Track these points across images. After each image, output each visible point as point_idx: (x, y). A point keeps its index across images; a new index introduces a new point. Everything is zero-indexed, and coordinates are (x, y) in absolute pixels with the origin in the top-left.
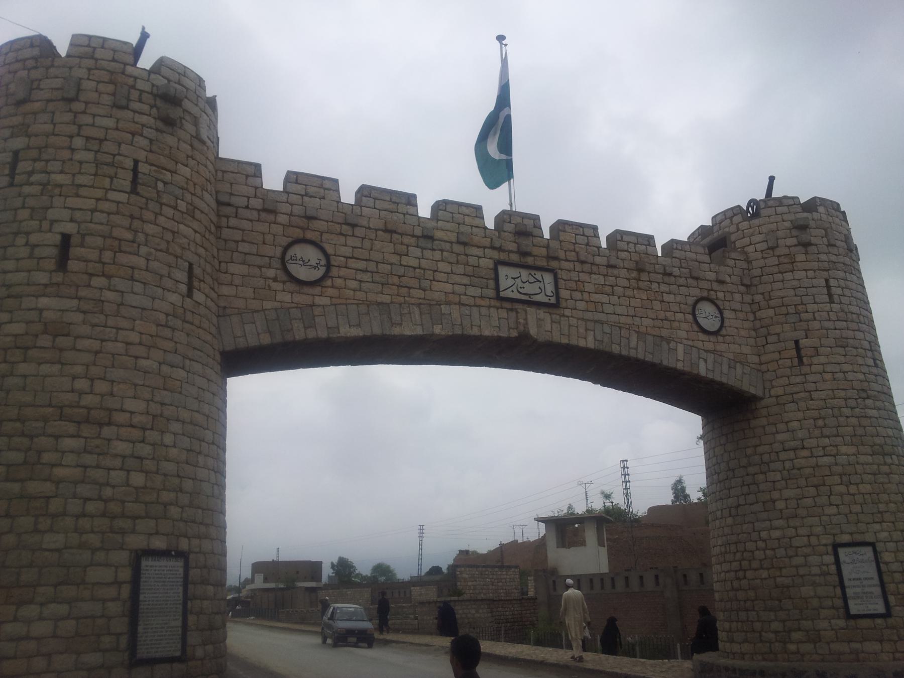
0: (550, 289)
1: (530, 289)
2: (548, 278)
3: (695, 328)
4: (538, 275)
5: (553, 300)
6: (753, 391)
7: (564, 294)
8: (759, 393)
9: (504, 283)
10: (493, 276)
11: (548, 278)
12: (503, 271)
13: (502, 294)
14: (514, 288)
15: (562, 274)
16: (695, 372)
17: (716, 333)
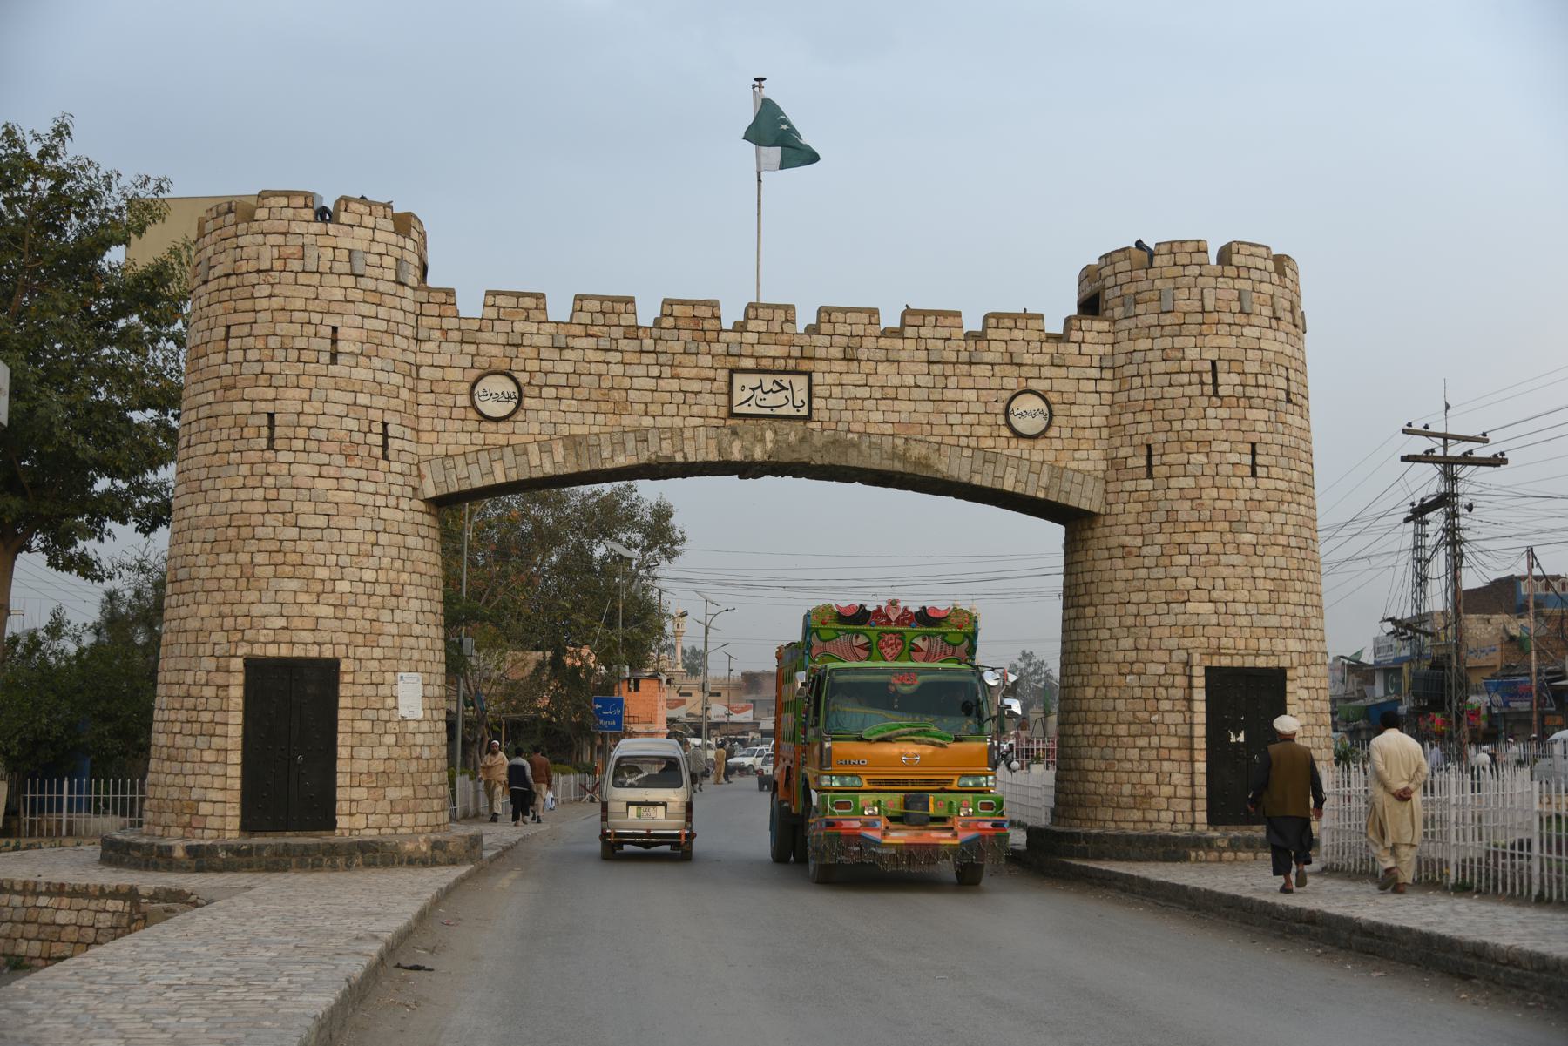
0: (801, 395)
1: (771, 400)
2: (800, 383)
3: (1006, 432)
4: (785, 380)
5: (804, 411)
6: (1084, 505)
7: (817, 403)
8: (1095, 507)
9: (739, 396)
10: (725, 390)
11: (800, 383)
12: (737, 377)
13: (736, 410)
14: (752, 402)
15: (817, 378)
16: (998, 486)
17: (1041, 435)
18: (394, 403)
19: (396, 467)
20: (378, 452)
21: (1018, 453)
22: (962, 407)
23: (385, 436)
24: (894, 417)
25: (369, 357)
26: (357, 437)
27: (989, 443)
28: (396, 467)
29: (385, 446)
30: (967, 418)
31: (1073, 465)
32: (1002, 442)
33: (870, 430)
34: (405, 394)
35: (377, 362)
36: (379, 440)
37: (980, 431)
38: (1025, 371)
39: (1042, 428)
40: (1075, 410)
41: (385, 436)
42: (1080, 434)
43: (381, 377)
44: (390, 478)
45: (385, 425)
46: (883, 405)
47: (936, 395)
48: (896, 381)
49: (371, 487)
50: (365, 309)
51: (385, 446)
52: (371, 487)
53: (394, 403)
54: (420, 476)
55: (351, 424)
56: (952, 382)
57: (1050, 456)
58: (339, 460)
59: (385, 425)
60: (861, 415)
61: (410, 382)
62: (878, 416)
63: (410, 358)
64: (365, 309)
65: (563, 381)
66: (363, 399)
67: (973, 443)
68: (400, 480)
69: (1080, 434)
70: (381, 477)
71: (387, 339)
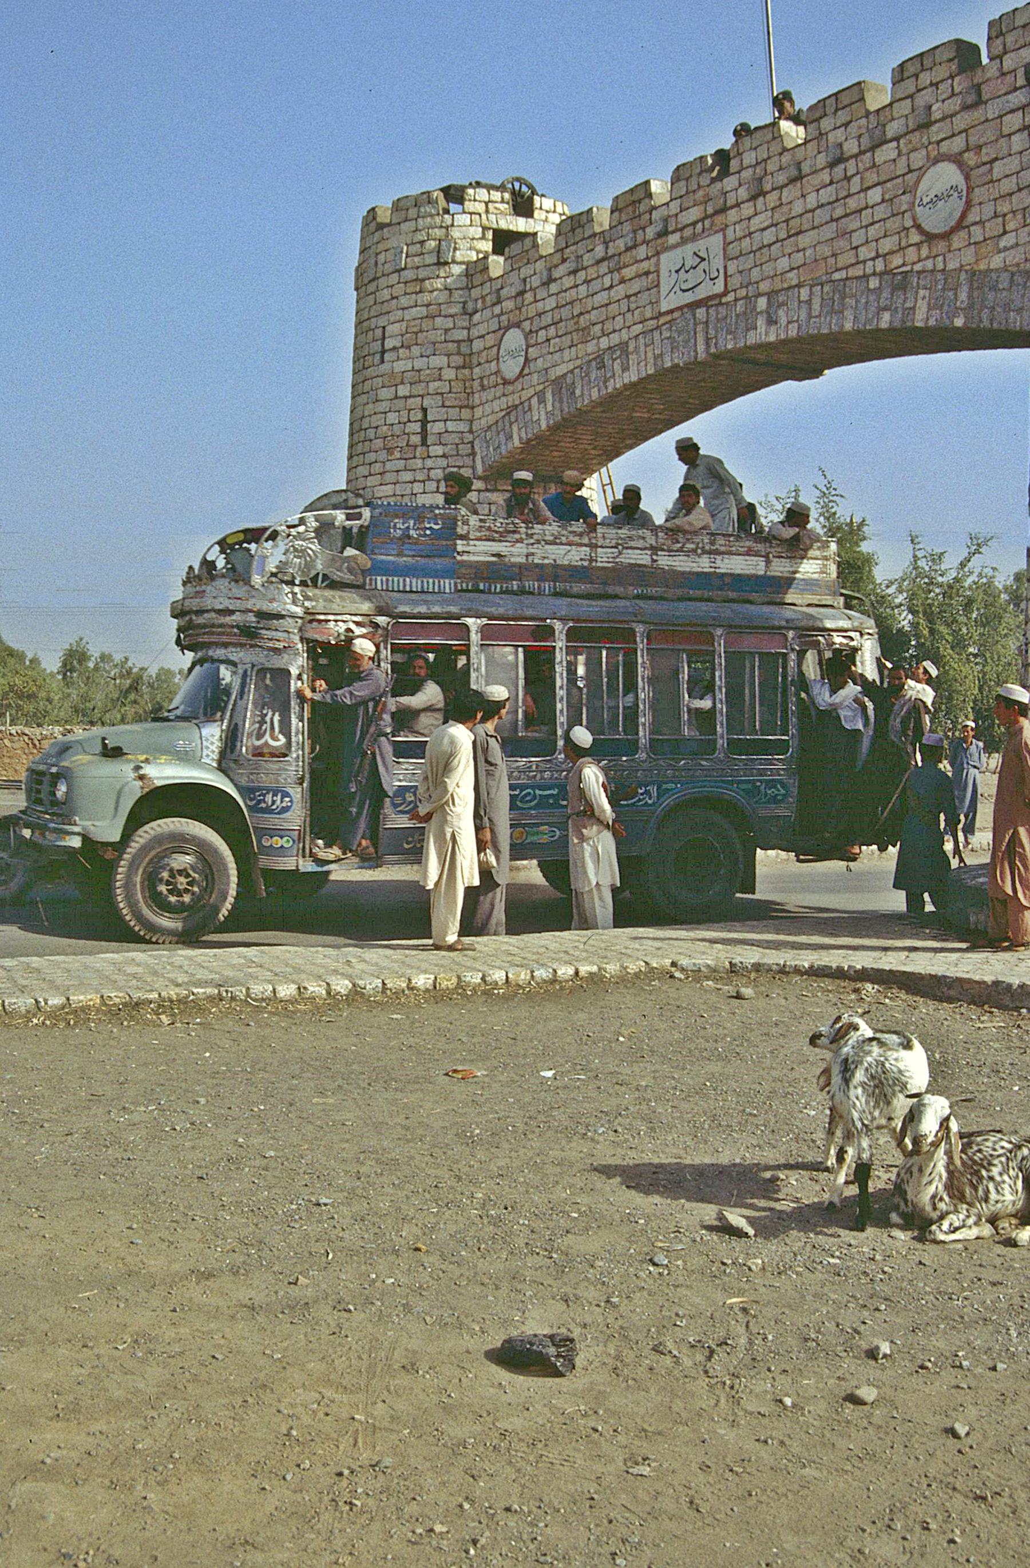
18: (433, 386)
19: (439, 450)
20: (416, 439)
21: (929, 264)
22: (866, 216)
23: (424, 422)
24: (798, 258)
25: (409, 347)
26: (397, 429)
27: (897, 261)
28: (439, 450)
29: (424, 434)
30: (872, 231)
31: (996, 262)
32: (911, 254)
33: (778, 286)
34: (449, 374)
35: (416, 350)
36: (417, 427)
37: (887, 245)
38: (937, 132)
39: (957, 215)
40: (998, 170)
41: (424, 422)
42: (1004, 207)
43: (419, 364)
44: (429, 463)
45: (425, 410)
46: (789, 246)
47: (839, 212)
48: (798, 208)
49: (407, 476)
50: (404, 301)
51: (424, 434)
52: (407, 476)
53: (433, 386)
54: (473, 454)
55: (392, 418)
56: (855, 184)
57: (968, 256)
58: (383, 455)
59: (425, 410)
60: (768, 269)
61: (458, 360)
62: (783, 264)
63: (462, 335)
64: (404, 301)
65: (547, 319)
66: (403, 391)
67: (880, 265)
68: (443, 462)
69: (1004, 207)
70: (419, 463)
71: (426, 324)
